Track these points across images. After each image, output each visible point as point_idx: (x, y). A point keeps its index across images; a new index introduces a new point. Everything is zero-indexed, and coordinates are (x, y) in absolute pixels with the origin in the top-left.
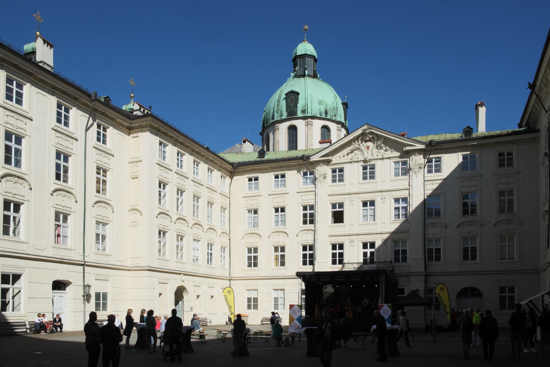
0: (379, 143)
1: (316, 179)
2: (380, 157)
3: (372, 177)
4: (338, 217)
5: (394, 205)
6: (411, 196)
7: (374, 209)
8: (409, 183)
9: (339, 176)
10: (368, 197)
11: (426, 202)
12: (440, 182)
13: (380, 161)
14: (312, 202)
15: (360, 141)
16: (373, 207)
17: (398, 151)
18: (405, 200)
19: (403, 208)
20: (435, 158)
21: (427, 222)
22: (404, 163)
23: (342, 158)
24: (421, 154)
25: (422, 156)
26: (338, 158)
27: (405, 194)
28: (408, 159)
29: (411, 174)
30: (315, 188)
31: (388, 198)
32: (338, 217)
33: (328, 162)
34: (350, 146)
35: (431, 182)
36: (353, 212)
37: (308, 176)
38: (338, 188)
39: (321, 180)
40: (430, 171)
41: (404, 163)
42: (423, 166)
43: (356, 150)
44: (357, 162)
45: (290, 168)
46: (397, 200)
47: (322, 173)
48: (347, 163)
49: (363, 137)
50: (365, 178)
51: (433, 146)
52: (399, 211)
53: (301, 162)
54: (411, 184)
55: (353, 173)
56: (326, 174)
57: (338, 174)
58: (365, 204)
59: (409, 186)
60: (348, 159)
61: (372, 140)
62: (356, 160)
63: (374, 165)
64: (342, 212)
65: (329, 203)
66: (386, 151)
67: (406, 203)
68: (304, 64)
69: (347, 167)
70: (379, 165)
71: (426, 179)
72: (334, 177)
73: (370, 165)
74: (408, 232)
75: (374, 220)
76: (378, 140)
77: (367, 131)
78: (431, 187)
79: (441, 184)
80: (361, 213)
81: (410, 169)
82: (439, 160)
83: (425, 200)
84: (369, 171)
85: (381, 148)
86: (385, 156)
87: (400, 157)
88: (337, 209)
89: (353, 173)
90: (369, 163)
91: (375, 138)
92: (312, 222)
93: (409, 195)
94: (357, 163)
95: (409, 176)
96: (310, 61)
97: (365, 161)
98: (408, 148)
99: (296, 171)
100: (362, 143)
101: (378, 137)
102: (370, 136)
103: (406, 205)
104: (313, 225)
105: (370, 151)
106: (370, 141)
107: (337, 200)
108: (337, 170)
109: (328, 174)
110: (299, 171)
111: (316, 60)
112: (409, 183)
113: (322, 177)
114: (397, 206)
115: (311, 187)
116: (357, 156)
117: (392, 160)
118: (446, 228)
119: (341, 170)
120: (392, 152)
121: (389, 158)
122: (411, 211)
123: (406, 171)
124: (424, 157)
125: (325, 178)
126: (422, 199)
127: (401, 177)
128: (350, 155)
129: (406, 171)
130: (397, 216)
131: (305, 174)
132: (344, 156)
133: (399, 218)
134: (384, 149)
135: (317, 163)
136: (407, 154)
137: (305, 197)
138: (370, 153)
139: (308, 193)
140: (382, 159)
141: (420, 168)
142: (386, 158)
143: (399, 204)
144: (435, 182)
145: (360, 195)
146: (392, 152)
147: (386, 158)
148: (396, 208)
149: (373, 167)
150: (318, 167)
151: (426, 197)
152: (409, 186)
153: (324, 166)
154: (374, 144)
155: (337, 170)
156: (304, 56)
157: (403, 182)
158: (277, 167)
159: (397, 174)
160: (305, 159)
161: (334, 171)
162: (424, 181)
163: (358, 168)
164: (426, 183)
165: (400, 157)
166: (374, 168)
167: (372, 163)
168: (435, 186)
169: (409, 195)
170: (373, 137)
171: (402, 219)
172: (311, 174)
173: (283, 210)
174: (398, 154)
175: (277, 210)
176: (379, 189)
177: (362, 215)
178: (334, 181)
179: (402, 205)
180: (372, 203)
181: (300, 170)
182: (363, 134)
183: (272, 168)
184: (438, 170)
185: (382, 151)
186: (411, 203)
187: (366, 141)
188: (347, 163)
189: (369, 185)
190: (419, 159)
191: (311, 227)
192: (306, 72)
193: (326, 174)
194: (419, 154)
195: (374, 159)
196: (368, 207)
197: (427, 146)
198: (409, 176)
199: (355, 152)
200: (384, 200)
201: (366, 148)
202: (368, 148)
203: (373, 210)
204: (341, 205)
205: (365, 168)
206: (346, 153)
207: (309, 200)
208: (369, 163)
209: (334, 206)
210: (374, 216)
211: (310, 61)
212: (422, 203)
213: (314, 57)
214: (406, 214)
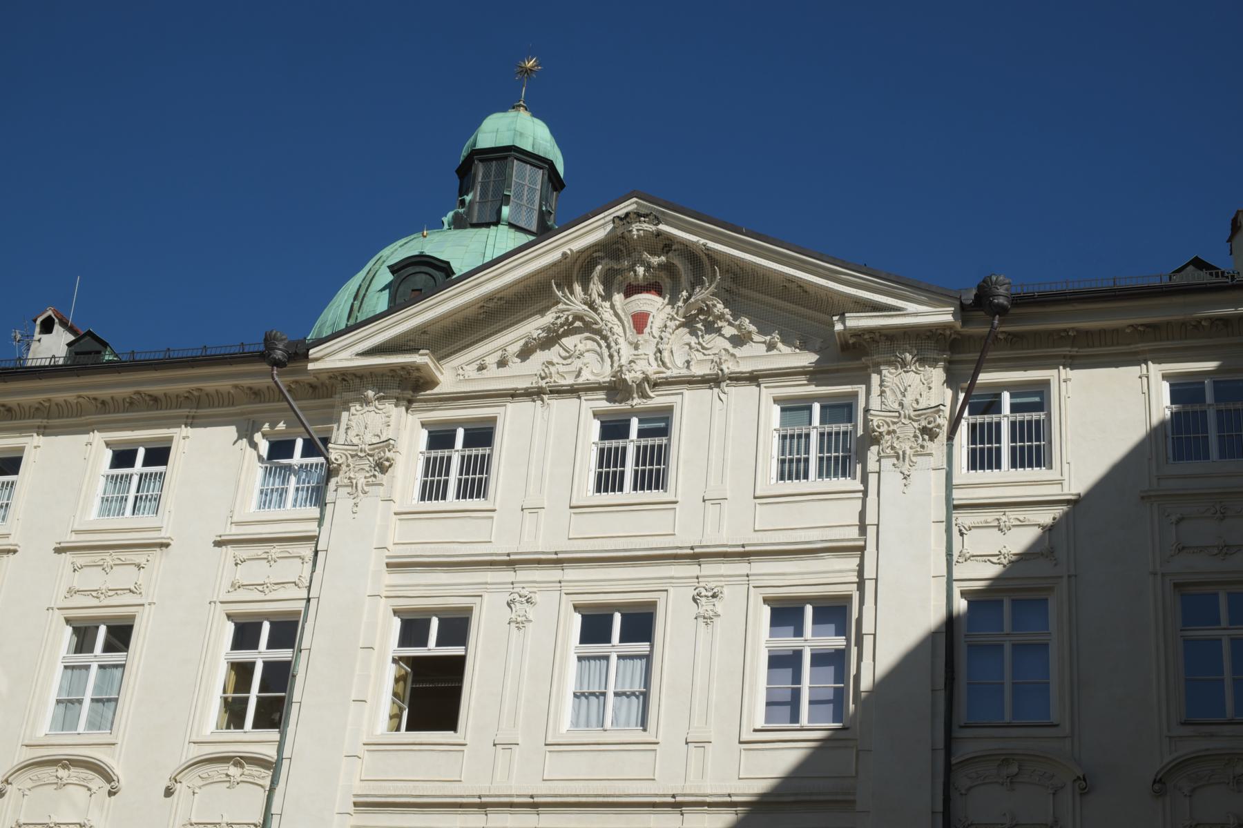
0: (701, 294)
1: (331, 472)
2: (698, 370)
3: (652, 479)
4: (432, 695)
5: (764, 638)
6: (869, 586)
7: (648, 658)
8: (862, 514)
9: (468, 465)
10: (617, 586)
11: (961, 630)
12: (1046, 517)
13: (705, 394)
14: (286, 600)
15: (596, 288)
16: (641, 647)
17: (805, 346)
18: (834, 611)
19: (819, 659)
20: (1017, 389)
21: (967, 748)
22: (840, 410)
23: (493, 370)
24: (933, 363)
25: (937, 374)
26: (471, 371)
27: (832, 575)
28: (861, 389)
29: (872, 465)
30: (321, 521)
31: (733, 596)
32: (432, 695)
33: (409, 387)
34: (542, 312)
35: (990, 516)
36: (522, 665)
37: (297, 459)
38: (456, 528)
39: (361, 480)
40: (983, 459)
41: (840, 410)
42: (944, 422)
43: (571, 332)
44: (573, 391)
45: (199, 410)
46: (785, 613)
47: (369, 438)
48: (513, 395)
49: (612, 265)
50: (608, 481)
51: (1001, 311)
52: (797, 678)
53: (257, 377)
54: (871, 518)
55: (543, 449)
56: (387, 444)
57: (464, 455)
58: (595, 626)
59: (863, 528)
60: (523, 374)
61: (666, 282)
62: (569, 381)
63: (665, 414)
64: (458, 664)
65: (384, 608)
66: (738, 341)
67: (842, 630)
68: (503, 179)
69: (512, 422)
70: (691, 410)
71: (959, 496)
72: (435, 468)
73: (644, 415)
74: (842, 803)
75: (644, 724)
76: (696, 282)
77: (639, 229)
78: (993, 548)
79: (1049, 531)
80: (570, 677)
81: (871, 438)
82: (1035, 399)
83: (951, 621)
84: (635, 446)
85: (711, 328)
86: (729, 367)
87: (815, 375)
88: (432, 648)
89: (543, 449)
90: (637, 402)
91: (678, 273)
92: (273, 714)
93: (861, 585)
94: (570, 404)
95: (865, 481)
96: (527, 180)
97: (616, 389)
98: (858, 321)
99: (232, 431)
100: (607, 297)
101: (700, 264)
102: (655, 260)
103: (839, 642)
104: (273, 734)
105: (649, 336)
106: (654, 287)
107: (437, 591)
108: (460, 433)
109: (403, 444)
110: (247, 433)
111: (555, 182)
112: (862, 514)
113: (367, 464)
114: (787, 642)
115: (295, 513)
116: (577, 364)
117: (768, 392)
118: (1084, 792)
119: (481, 435)
120: (771, 347)
121: (753, 378)
122: (866, 683)
123: (847, 456)
124: (951, 381)
125: (382, 467)
126: (933, 616)
127: (814, 483)
128: (539, 357)
129: (847, 456)
130: (784, 706)
131: (281, 449)
132: (502, 363)
133: (795, 717)
134: (729, 331)
135: (348, 386)
136: (856, 355)
137: (256, 572)
138: (649, 349)
139: (276, 550)
140: (712, 381)
141: (929, 433)
142: (737, 379)
143: (799, 632)
144: (1012, 515)
145: (572, 574)
146: (771, 347)
147: (737, 379)
148: (777, 661)
149: (659, 425)
150: (355, 408)
151: (961, 605)
152: (863, 528)
153: (389, 407)
154: (672, 302)
155: (460, 433)
156: (505, 154)
157: (825, 509)
158: (131, 404)
159: (792, 469)
160: (279, 354)
161: (440, 438)
162: (953, 507)
163: (575, 429)
164: (964, 519)
165: (815, 375)
166: (665, 432)
167: (658, 399)
168: (1020, 540)
169: (861, 585)
170: (668, 268)
171: (814, 726)
172: (310, 450)
173: (120, 636)
174: (807, 359)
175: (83, 636)
176: (686, 538)
177: (571, 686)
178: (434, 490)
179: (813, 638)
180: (640, 624)
181: (256, 427)
182: (615, 249)
183: (104, 406)
184: (1033, 449)
185: (717, 343)
186: (867, 627)
187: (630, 291)
188: (513, 395)
189: (633, 521)
190: (925, 387)
191: (262, 742)
192: (506, 211)
193: (387, 444)
194: (923, 361)
195: (668, 382)
196: (615, 645)
197: (964, 311)
198: (865, 481)
199: (568, 341)
200: (706, 606)
201: (629, 323)
202: (640, 321)
203: (639, 665)
204: (456, 626)
205: (613, 428)
206: (516, 348)
207: (273, 584)
208: (637, 402)
209: (413, 630)
210: (645, 696)
211: (527, 180)
212: (933, 636)
213: (551, 165)
214: (840, 695)
